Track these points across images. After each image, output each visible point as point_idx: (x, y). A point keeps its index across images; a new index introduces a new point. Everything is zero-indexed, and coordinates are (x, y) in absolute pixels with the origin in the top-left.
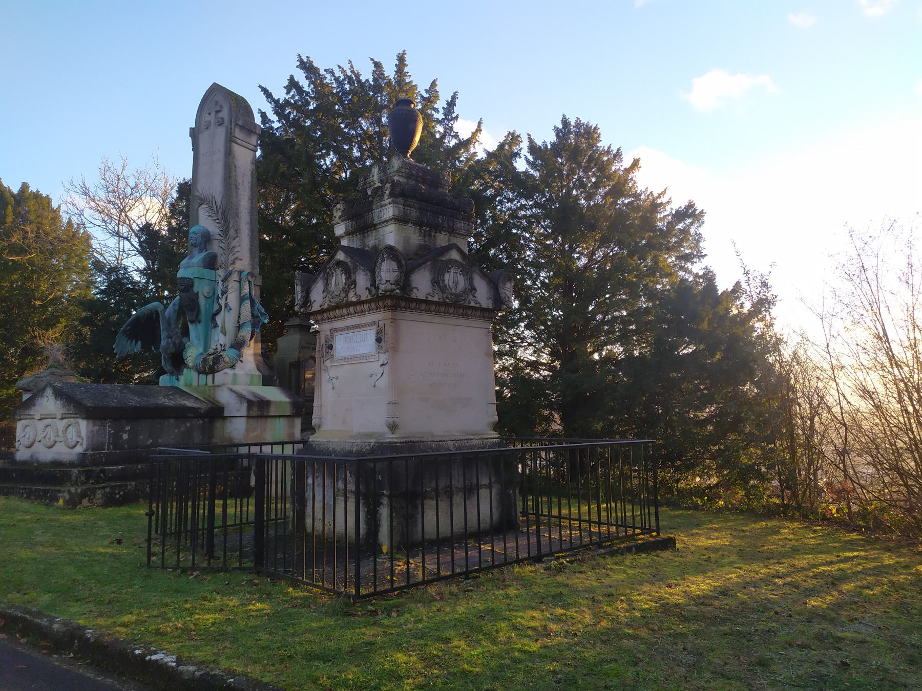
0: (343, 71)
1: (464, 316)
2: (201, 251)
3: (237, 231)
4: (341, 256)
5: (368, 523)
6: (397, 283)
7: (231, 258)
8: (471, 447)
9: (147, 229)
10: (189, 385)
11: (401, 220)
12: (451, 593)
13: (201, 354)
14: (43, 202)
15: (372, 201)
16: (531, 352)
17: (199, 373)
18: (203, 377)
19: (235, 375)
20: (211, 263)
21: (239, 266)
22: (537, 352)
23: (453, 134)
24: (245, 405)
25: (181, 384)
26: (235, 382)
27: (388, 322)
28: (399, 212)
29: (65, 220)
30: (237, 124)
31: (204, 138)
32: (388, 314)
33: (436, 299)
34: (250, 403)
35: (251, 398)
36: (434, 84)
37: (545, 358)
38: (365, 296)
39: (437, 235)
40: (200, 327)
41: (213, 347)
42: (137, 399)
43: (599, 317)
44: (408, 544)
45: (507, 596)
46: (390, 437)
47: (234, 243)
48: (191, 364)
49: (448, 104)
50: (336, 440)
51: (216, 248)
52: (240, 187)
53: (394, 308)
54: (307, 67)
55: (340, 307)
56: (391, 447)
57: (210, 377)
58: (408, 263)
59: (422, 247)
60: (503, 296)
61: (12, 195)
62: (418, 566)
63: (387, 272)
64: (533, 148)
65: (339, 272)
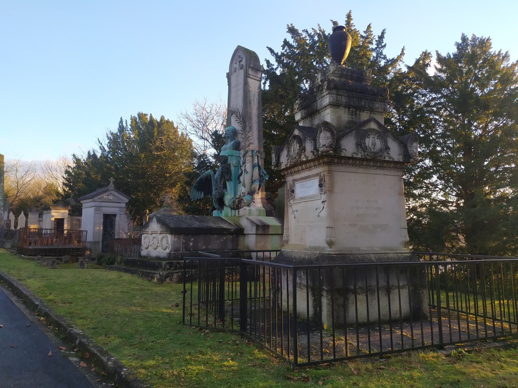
0: (315, 31)
1: (381, 167)
2: (232, 141)
3: (250, 128)
4: (296, 132)
5: (315, 308)
6: (330, 146)
7: (247, 143)
8: (388, 259)
9: (215, 133)
10: (226, 216)
11: (334, 105)
12: (367, 369)
13: (232, 198)
14: (169, 123)
15: (316, 95)
16: (442, 194)
17: (232, 209)
18: (233, 211)
19: (250, 210)
20: (237, 147)
21: (252, 147)
22: (446, 194)
23: (382, 56)
24: (255, 227)
25: (223, 216)
26: (250, 214)
27: (326, 173)
28: (333, 99)
29: (180, 133)
30: (250, 67)
31: (233, 77)
32: (326, 168)
33: (359, 156)
34: (258, 226)
35: (259, 223)
36: (369, 27)
37: (453, 198)
38: (310, 156)
39: (361, 113)
40: (232, 183)
41: (239, 194)
42: (198, 224)
43: (493, 169)
44: (341, 326)
45: (412, 378)
46: (328, 250)
47: (249, 134)
48: (227, 204)
49: (379, 37)
50: (296, 251)
51: (240, 138)
52: (252, 102)
53: (330, 163)
54: (292, 30)
55: (297, 165)
56: (329, 257)
57: (237, 211)
58: (338, 134)
59: (349, 122)
60: (411, 152)
61: (157, 122)
62: (346, 343)
63: (324, 139)
64: (440, 60)
65: (295, 143)
